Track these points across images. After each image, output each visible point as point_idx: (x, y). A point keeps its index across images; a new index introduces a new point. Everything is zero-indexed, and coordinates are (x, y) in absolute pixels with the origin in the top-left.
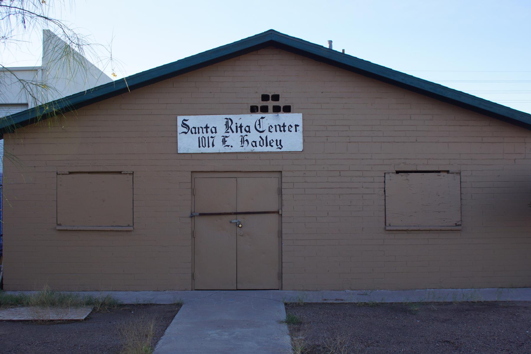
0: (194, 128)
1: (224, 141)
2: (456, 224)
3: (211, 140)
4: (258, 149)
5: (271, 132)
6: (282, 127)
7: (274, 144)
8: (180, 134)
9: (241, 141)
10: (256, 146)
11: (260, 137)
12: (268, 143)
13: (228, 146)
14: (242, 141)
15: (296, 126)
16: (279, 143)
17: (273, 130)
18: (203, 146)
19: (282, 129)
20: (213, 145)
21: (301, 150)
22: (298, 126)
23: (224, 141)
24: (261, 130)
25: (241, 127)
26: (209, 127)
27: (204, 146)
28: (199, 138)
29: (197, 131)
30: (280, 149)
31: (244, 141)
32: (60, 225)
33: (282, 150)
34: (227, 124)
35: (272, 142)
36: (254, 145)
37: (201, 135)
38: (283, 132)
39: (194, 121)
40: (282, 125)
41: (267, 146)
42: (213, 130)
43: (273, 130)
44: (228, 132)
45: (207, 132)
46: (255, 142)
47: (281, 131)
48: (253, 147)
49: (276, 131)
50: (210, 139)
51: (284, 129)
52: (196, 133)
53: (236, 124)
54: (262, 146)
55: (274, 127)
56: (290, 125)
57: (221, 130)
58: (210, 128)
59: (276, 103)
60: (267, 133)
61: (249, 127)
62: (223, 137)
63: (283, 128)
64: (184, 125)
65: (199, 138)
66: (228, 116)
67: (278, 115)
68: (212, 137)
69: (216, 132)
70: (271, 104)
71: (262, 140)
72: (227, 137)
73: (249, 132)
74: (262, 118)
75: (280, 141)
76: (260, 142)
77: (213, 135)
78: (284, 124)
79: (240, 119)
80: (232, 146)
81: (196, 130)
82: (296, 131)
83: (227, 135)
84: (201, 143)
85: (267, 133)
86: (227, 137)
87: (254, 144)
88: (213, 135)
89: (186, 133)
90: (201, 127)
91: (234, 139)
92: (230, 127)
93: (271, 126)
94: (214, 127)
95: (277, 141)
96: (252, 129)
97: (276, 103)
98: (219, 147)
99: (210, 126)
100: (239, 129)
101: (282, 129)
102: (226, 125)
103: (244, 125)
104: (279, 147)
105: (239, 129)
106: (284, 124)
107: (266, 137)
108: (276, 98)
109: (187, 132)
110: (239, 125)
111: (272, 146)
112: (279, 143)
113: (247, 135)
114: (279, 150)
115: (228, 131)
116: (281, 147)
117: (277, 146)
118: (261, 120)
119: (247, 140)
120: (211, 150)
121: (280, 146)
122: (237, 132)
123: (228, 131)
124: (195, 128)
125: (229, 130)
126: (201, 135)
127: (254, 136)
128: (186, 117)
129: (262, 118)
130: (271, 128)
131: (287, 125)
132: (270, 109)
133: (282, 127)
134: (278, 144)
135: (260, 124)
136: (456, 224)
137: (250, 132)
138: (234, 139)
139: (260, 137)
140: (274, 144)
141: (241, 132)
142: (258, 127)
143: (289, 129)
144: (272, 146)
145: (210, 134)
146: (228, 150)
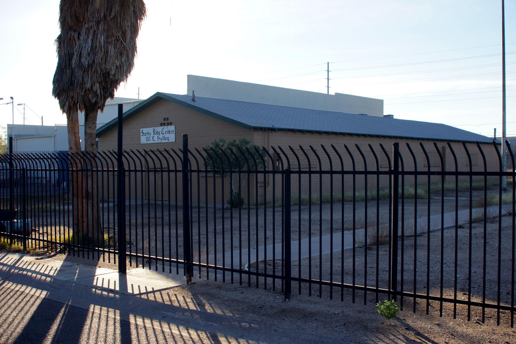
1: (153, 138)
4: (163, 141)
7: (167, 139)
15: (173, 131)
17: (166, 133)
23: (153, 138)
34: (154, 132)
39: (145, 130)
43: (166, 133)
57: (152, 133)
70: (166, 122)
73: (160, 134)
83: (154, 136)
88: (150, 136)
97: (168, 122)
98: (151, 142)
108: (168, 119)
126: (147, 136)
128: (143, 129)
131: (170, 131)
132: (166, 124)
140: (167, 139)
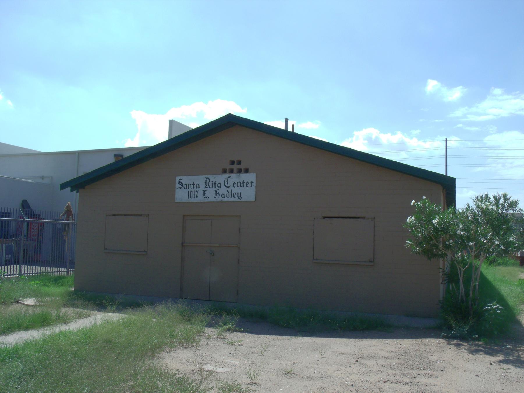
0: (186, 184)
1: (204, 194)
2: (369, 260)
3: (196, 193)
4: (226, 199)
5: (235, 187)
6: (242, 183)
7: (236, 196)
8: (177, 189)
9: (215, 194)
10: (224, 197)
11: (227, 191)
12: (231, 194)
13: (206, 197)
14: (216, 194)
15: (252, 182)
16: (240, 195)
17: (236, 185)
18: (190, 197)
19: (242, 185)
20: (197, 197)
21: (254, 200)
22: (253, 182)
23: (204, 194)
24: (228, 186)
25: (215, 184)
26: (195, 184)
27: (191, 197)
28: (188, 191)
29: (187, 187)
30: (240, 199)
31: (216, 194)
33: (242, 200)
34: (206, 182)
35: (235, 194)
36: (223, 197)
37: (190, 190)
38: (242, 187)
39: (186, 180)
40: (242, 182)
41: (231, 197)
42: (198, 186)
44: (207, 188)
45: (194, 188)
46: (224, 194)
47: (241, 186)
48: (223, 198)
49: (238, 186)
50: (195, 192)
51: (243, 185)
52: (186, 188)
53: (212, 181)
54: (228, 197)
55: (237, 183)
56: (248, 182)
57: (203, 186)
58: (196, 185)
59: (239, 166)
60: (232, 188)
61: (220, 183)
62: (203, 191)
63: (242, 184)
64: (180, 183)
65: (188, 191)
66: (239, 200)
67: (239, 175)
68: (196, 191)
69: (199, 188)
70: (235, 167)
71: (228, 193)
72: (206, 191)
73: (220, 187)
74: (229, 177)
75: (240, 193)
76: (227, 194)
78: (243, 181)
79: (215, 178)
80: (209, 198)
81: (186, 187)
82: (251, 186)
84: (190, 195)
85: (232, 188)
86: (206, 191)
87: (223, 196)
88: (198, 189)
89: (180, 188)
90: (190, 184)
91: (211, 192)
92: (208, 184)
93: (234, 183)
94: (198, 184)
95: (238, 193)
96: (222, 185)
97: (239, 166)
98: (200, 198)
99: (196, 183)
100: (214, 185)
101: (242, 185)
102: (205, 182)
103: (217, 183)
104: (239, 198)
105: (214, 185)
106: (243, 181)
107: (231, 191)
108: (239, 162)
109: (181, 187)
110: (214, 183)
111: (235, 197)
112: (240, 195)
113: (218, 190)
114: (239, 200)
115: (206, 187)
116: (240, 198)
117: (238, 197)
118: (228, 178)
119: (218, 193)
120: (195, 200)
121: (240, 198)
122: (212, 187)
123: (206, 187)
124: (186, 185)
125: (208, 186)
126: (190, 190)
127: (223, 190)
128: (181, 178)
129: (229, 177)
130: (234, 184)
131: (245, 182)
132: (235, 171)
133: (242, 183)
134: (239, 196)
135: (227, 182)
136: (369, 260)
137: (221, 188)
138: (211, 192)
139: (227, 191)
140: (236, 196)
141: (215, 187)
142: (226, 184)
143: (246, 185)
144: (235, 197)
145: (195, 189)
146: (206, 200)
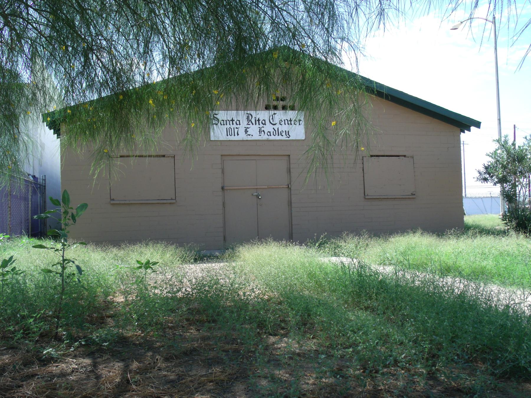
1: (246, 131)
3: (236, 130)
4: (272, 138)
7: (284, 134)
9: (259, 131)
10: (270, 135)
11: (273, 128)
13: (250, 135)
14: (260, 131)
17: (283, 123)
19: (289, 122)
20: (238, 134)
22: (301, 120)
23: (246, 131)
25: (259, 120)
29: (225, 123)
30: (289, 138)
32: (113, 200)
35: (282, 132)
36: (269, 135)
37: (228, 126)
40: (289, 120)
41: (278, 135)
42: (238, 123)
43: (283, 123)
44: (249, 124)
45: (233, 124)
46: (270, 132)
47: (288, 124)
49: (285, 124)
50: (235, 129)
52: (224, 125)
53: (255, 118)
55: (284, 121)
57: (244, 123)
61: (265, 120)
68: (237, 128)
69: (240, 124)
70: (281, 103)
74: (275, 114)
75: (288, 132)
77: (238, 126)
80: (252, 135)
83: (248, 126)
87: (269, 134)
88: (238, 126)
91: (254, 130)
92: (251, 120)
95: (286, 131)
96: (267, 122)
98: (242, 136)
100: (257, 122)
101: (289, 122)
103: (261, 119)
105: (257, 122)
110: (257, 119)
111: (282, 136)
112: (288, 133)
113: (263, 127)
114: (287, 139)
115: (249, 123)
119: (263, 131)
120: (236, 138)
121: (288, 136)
122: (256, 124)
123: (249, 123)
125: (250, 123)
126: (228, 126)
127: (268, 128)
132: (280, 107)
134: (287, 134)
135: (273, 119)
138: (254, 130)
139: (273, 128)
140: (284, 134)
141: (259, 124)
142: (271, 121)
144: (282, 136)
145: (235, 126)
146: (249, 138)
